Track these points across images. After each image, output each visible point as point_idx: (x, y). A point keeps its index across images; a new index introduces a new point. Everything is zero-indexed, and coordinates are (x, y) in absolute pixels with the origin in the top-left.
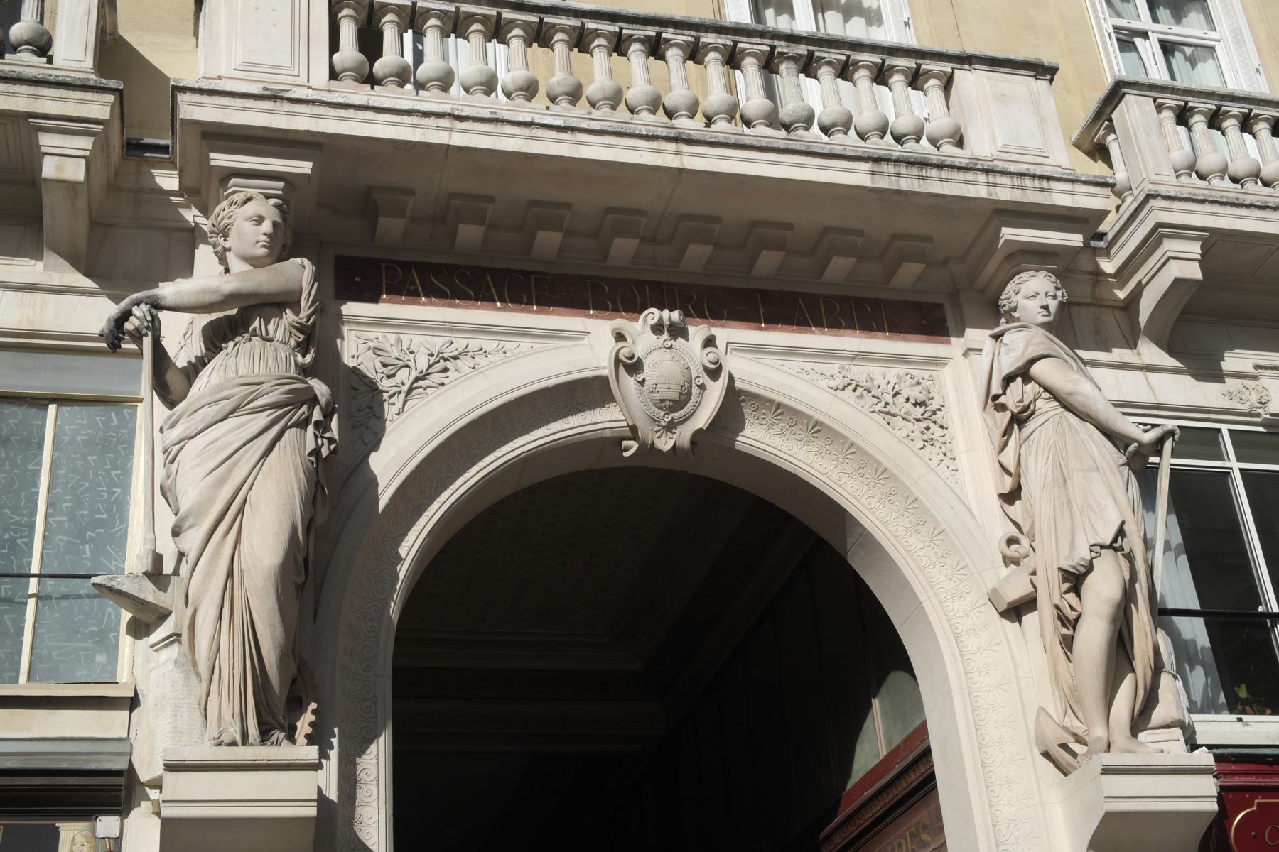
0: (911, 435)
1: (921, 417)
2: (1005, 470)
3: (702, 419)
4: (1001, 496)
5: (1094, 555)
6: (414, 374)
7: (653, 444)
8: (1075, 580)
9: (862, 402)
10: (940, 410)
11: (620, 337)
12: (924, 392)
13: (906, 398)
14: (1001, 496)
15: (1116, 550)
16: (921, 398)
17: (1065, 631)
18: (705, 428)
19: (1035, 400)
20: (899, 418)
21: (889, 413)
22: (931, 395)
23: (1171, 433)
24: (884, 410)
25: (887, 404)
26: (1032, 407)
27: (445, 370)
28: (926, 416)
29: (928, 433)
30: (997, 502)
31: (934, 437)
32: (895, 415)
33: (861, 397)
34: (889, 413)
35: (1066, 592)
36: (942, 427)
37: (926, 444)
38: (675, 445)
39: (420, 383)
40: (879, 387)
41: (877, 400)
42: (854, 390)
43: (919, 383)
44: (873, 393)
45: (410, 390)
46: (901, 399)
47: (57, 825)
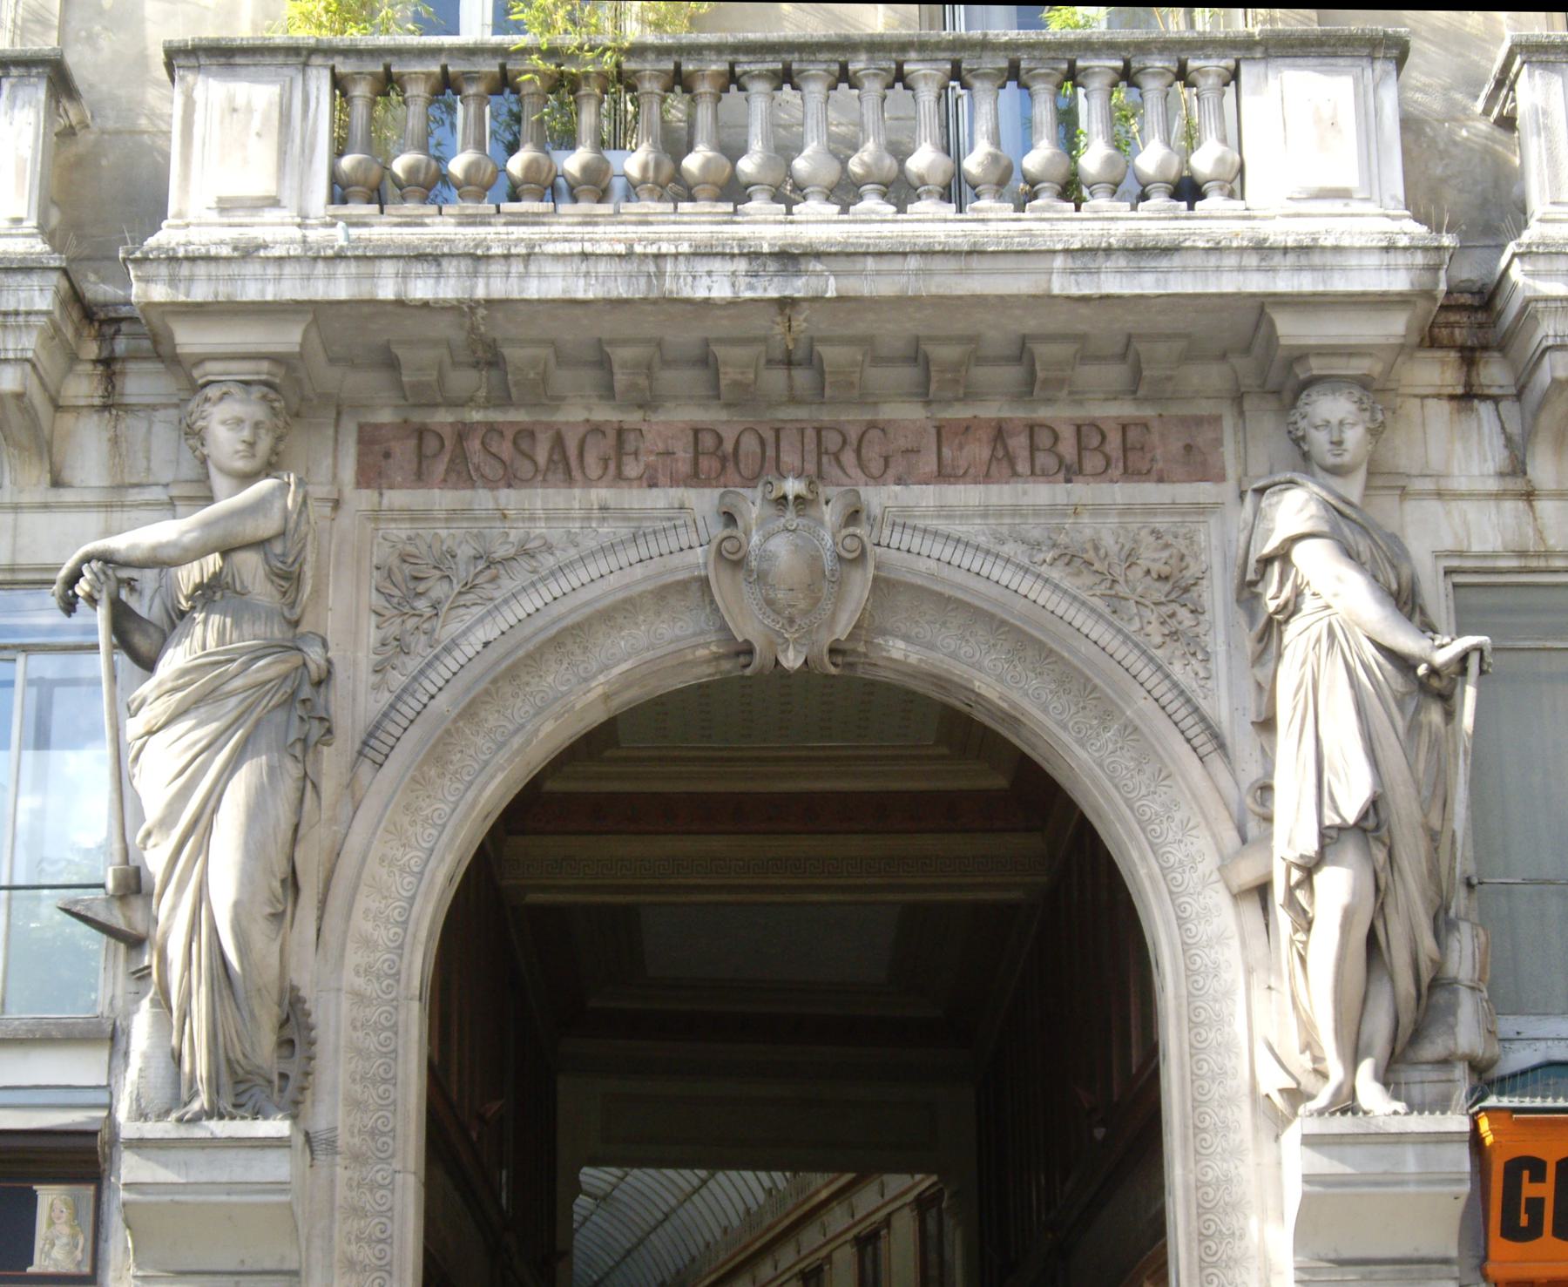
1: (1163, 599)
3: (842, 630)
6: (457, 588)
7: (777, 662)
9: (1079, 581)
10: (1195, 584)
11: (730, 518)
12: (1172, 562)
13: (1145, 569)
14: (1253, 723)
15: (1365, 831)
16: (1165, 570)
18: (843, 639)
20: (1132, 602)
22: (1184, 564)
23: (1479, 649)
24: (1108, 592)
26: (1291, 607)
27: (493, 579)
28: (1173, 596)
29: (1173, 622)
31: (1181, 628)
33: (1078, 574)
34: (1116, 596)
37: (1168, 639)
40: (1106, 555)
41: (1100, 577)
42: (1068, 564)
43: (1167, 546)
44: (1094, 568)
45: (451, 609)
46: (1137, 573)
47: (35, 1187)
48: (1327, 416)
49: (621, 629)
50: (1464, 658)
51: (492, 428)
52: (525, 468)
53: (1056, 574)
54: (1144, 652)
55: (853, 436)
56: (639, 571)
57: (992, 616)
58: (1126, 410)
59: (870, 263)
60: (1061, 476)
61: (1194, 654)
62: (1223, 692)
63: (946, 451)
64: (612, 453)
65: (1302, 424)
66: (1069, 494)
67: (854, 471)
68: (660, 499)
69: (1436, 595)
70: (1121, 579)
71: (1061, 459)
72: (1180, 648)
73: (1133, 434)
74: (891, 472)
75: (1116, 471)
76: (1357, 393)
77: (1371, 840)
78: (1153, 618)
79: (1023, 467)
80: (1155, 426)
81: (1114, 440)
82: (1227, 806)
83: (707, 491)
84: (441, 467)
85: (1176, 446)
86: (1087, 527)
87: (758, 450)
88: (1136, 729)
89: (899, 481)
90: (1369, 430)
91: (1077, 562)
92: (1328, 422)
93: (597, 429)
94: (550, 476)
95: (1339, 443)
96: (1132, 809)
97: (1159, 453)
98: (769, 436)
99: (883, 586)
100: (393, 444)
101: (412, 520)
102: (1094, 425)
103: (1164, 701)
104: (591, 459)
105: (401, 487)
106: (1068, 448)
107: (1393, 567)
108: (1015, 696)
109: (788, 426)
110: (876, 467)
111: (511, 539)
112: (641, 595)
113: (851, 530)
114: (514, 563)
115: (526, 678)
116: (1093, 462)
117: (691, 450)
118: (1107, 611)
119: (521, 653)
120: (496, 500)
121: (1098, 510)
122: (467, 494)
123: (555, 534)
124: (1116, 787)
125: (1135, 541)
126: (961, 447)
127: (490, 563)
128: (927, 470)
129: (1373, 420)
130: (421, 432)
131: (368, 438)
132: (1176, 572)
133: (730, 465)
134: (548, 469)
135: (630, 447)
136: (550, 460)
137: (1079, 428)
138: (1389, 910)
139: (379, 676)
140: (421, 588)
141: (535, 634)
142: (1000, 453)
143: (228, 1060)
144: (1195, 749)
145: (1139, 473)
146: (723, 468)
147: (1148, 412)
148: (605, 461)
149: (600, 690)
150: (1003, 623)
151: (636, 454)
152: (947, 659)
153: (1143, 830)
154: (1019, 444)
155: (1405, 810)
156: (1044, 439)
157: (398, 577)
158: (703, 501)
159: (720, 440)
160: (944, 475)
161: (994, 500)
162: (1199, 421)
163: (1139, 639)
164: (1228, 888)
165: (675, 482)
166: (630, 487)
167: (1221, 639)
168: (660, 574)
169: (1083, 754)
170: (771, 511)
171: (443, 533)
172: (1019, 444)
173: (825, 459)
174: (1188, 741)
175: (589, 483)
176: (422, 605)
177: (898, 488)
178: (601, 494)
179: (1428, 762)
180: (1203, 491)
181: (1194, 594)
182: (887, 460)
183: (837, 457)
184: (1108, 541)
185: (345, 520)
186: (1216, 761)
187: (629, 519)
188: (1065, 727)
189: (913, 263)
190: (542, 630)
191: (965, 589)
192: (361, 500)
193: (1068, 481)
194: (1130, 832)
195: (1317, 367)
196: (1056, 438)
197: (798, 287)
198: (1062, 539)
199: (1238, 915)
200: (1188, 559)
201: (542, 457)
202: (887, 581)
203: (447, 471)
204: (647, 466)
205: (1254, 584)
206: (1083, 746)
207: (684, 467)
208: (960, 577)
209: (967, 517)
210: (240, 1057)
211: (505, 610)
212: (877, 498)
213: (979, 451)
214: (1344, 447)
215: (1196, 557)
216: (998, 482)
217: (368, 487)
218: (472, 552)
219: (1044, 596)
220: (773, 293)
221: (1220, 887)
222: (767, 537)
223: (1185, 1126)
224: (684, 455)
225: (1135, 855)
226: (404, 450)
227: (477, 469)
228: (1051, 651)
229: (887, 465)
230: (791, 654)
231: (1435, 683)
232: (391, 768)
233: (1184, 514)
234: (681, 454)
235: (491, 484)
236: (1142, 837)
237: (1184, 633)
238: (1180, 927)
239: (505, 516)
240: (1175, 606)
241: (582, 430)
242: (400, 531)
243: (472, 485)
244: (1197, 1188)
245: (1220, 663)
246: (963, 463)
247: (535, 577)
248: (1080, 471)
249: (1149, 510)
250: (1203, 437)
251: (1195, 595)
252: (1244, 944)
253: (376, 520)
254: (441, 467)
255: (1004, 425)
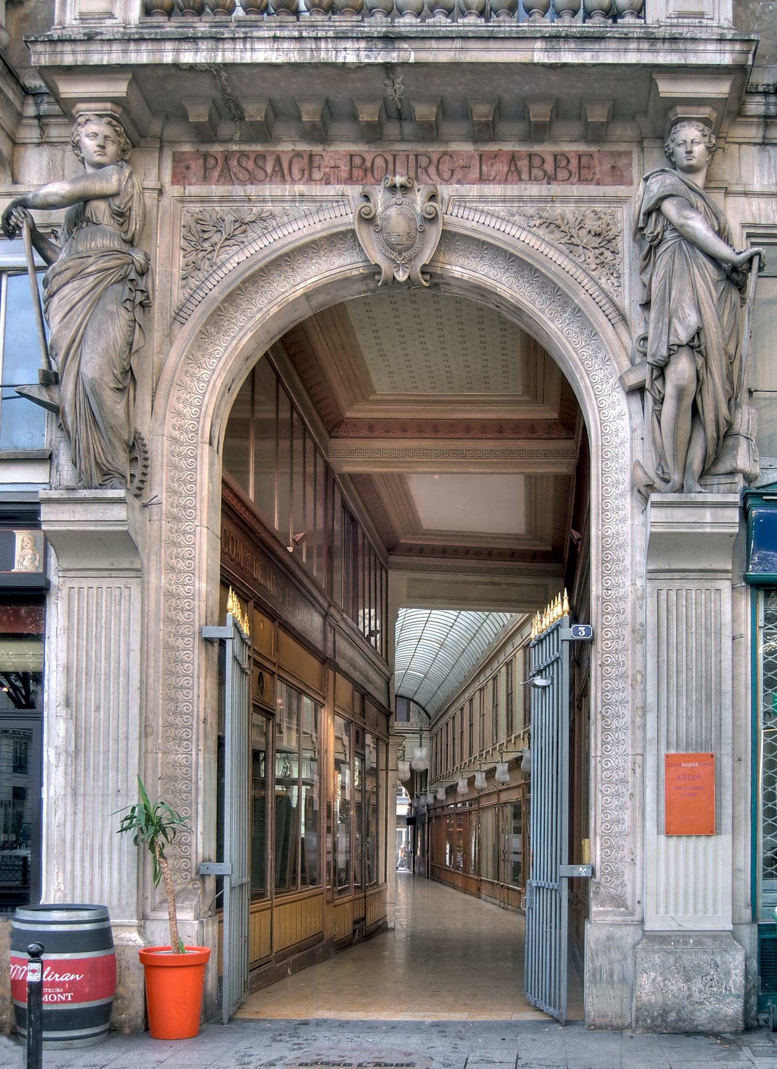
0: (589, 261)
2: (645, 285)
4: (640, 305)
5: (672, 352)
6: (224, 236)
8: (661, 370)
9: (553, 236)
14: (640, 305)
15: (692, 347)
16: (599, 230)
17: (656, 408)
19: (664, 232)
21: (572, 244)
25: (572, 236)
26: (660, 237)
27: (244, 232)
28: (602, 244)
29: (602, 258)
30: (639, 309)
32: (578, 245)
33: (552, 232)
34: (572, 244)
35: (656, 378)
36: (613, 252)
38: (409, 277)
39: (227, 243)
41: (564, 234)
43: (600, 218)
46: (583, 232)
48: (684, 138)
49: (312, 259)
50: (750, 260)
51: (243, 154)
52: (261, 175)
53: (541, 232)
54: (587, 274)
55: (435, 158)
56: (319, 226)
57: (506, 251)
58: (582, 148)
59: (434, 44)
60: (545, 180)
61: (612, 274)
62: (627, 293)
63: (484, 168)
64: (306, 167)
65: (672, 145)
66: (549, 190)
67: (435, 177)
68: (332, 190)
69: (737, 234)
70: (575, 235)
71: (545, 172)
72: (605, 271)
73: (584, 160)
74: (455, 177)
75: (574, 179)
76: (702, 126)
77: (696, 354)
78: (591, 255)
79: (525, 176)
80: (596, 156)
81: (574, 163)
82: (625, 349)
83: (357, 186)
84: (216, 174)
85: (607, 166)
86: (558, 209)
87: (384, 166)
88: (580, 310)
89: (459, 182)
90: (708, 148)
91: (552, 226)
92: (685, 142)
93: (298, 155)
94: (273, 179)
95: (689, 152)
96: (577, 353)
97: (598, 170)
98: (390, 158)
99: (449, 238)
100: (191, 162)
101: (202, 202)
102: (563, 155)
103: (594, 296)
104: (295, 170)
105: (195, 184)
106: (549, 167)
107: (717, 218)
108: (518, 296)
109: (401, 153)
110: (446, 175)
111: (254, 212)
112: (320, 239)
113: (430, 203)
114: (255, 224)
115: (262, 284)
116: (562, 174)
117: (348, 165)
118: (567, 252)
119: (256, 268)
120: (245, 191)
121: (565, 200)
122: (230, 187)
123: (277, 209)
124: (569, 342)
125: (584, 216)
126: (492, 165)
127: (242, 224)
128: (474, 176)
129: (710, 142)
130: (206, 156)
131: (177, 159)
132: (604, 232)
133: (369, 173)
134: (272, 175)
135: (316, 164)
136: (274, 170)
137: (555, 156)
138: (704, 392)
139: (185, 281)
140: (206, 236)
141: (264, 258)
142: (513, 169)
143: (97, 463)
144: (610, 320)
145: (587, 180)
146: (366, 175)
147: (593, 149)
148: (303, 171)
149: (301, 291)
150: (512, 255)
151: (319, 167)
152: (483, 277)
153: (583, 363)
154: (523, 164)
155: (713, 337)
156: (537, 162)
157: (194, 231)
158: (354, 191)
159: (364, 160)
160: (482, 179)
161: (509, 193)
162: (620, 154)
163: (584, 266)
164: (624, 389)
165: (339, 182)
166: (316, 184)
167: (627, 266)
168: (330, 228)
169: (553, 326)
170: (388, 195)
171: (218, 209)
172: (523, 164)
173: (419, 170)
174: (607, 316)
175: (293, 182)
176: (206, 245)
177: (458, 186)
178: (300, 188)
179: (729, 318)
180: (621, 190)
181: (614, 243)
182: (452, 171)
183: (426, 170)
184: (569, 216)
185: (166, 201)
186: (622, 329)
187: (315, 201)
188: (543, 312)
189: (458, 44)
190: (267, 256)
191: (492, 237)
192: (173, 191)
193: (549, 183)
194: (576, 365)
195: (681, 112)
196: (543, 161)
197: (394, 57)
198: (545, 214)
199: (629, 403)
200: (611, 226)
201: (269, 170)
202: (450, 232)
203: (219, 176)
204: (325, 174)
205: (642, 229)
206: (552, 321)
207: (344, 174)
208: (489, 231)
209: (495, 202)
210: (105, 462)
211: (249, 247)
212: (446, 191)
213: (502, 167)
214: (693, 155)
215: (616, 224)
216: (511, 183)
217: (178, 184)
218: (233, 219)
219: (533, 242)
220: (380, 60)
221: (620, 390)
222: (387, 207)
223: (598, 509)
224: (344, 168)
225: (578, 377)
226: (196, 166)
227: (235, 175)
228: (536, 270)
229: (452, 174)
230: (401, 273)
231: (735, 276)
232: (189, 325)
233: (610, 202)
234: (343, 168)
235: (243, 183)
236: (582, 367)
237: (607, 263)
238: (599, 412)
239: (250, 200)
240: (602, 250)
241: (291, 155)
242: (196, 208)
243: (232, 182)
244: (603, 538)
245: (626, 279)
246: (493, 174)
247: (265, 231)
248: (556, 179)
249: (591, 200)
250: (622, 162)
251: (614, 244)
252: (631, 418)
253: (182, 201)
254: (216, 174)
255: (516, 155)
